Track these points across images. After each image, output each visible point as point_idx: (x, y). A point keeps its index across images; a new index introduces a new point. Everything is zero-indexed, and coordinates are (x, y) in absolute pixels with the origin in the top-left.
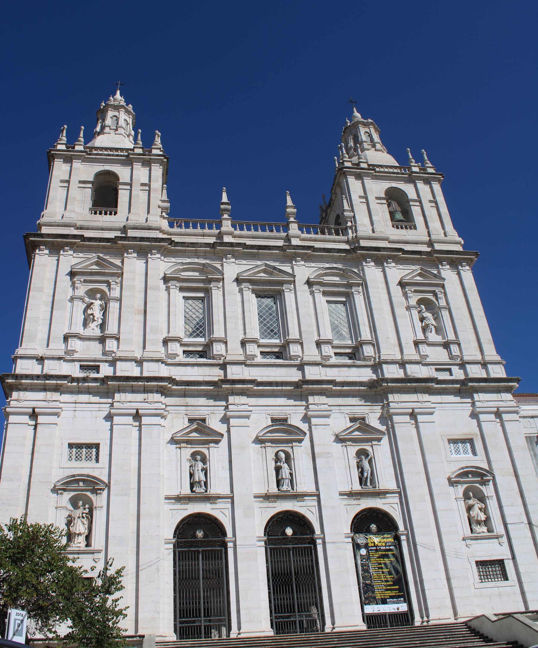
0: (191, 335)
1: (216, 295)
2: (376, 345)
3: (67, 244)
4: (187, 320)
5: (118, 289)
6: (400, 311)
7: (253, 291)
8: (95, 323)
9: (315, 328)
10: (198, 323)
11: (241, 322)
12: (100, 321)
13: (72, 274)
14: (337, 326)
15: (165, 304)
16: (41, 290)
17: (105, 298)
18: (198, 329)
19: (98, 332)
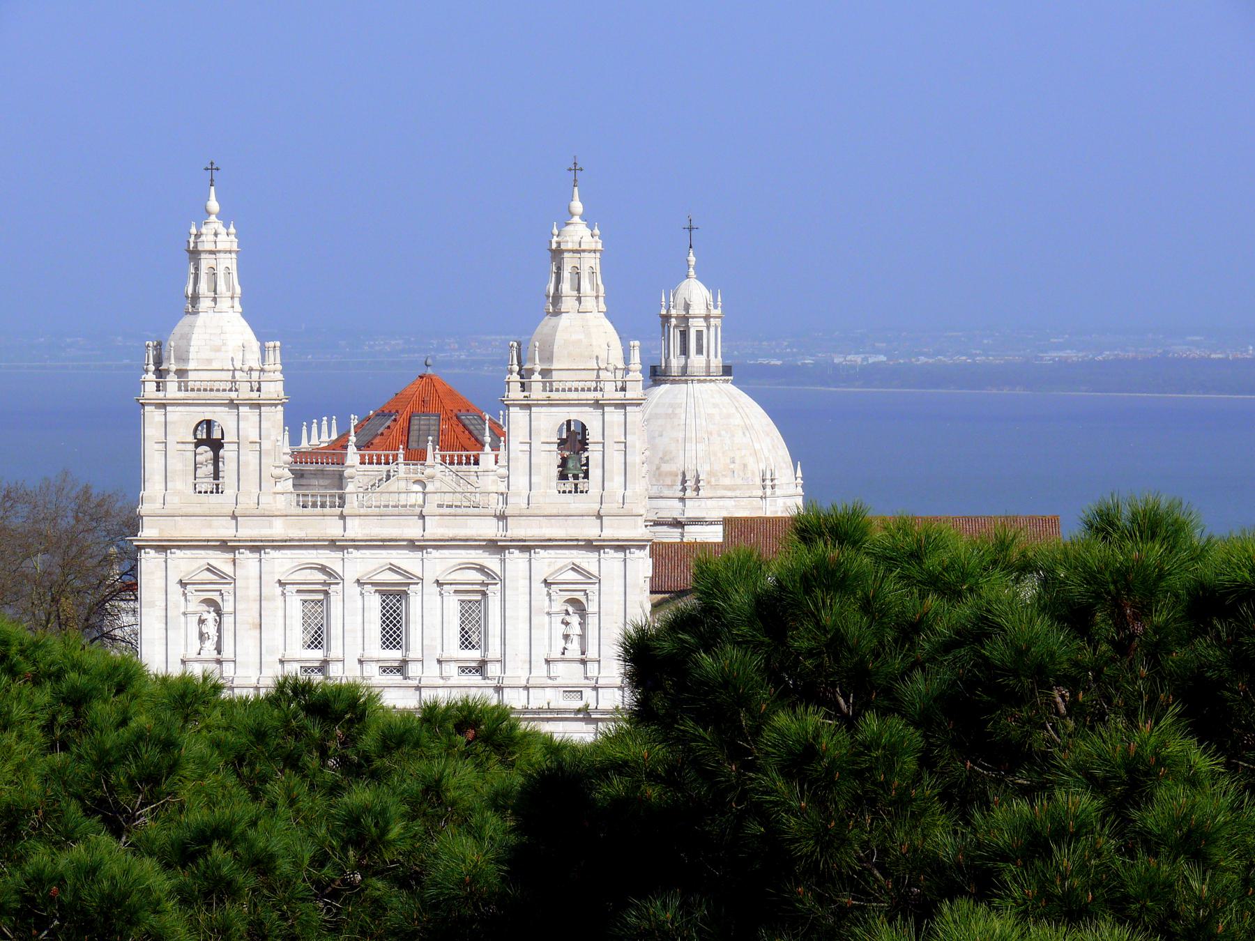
0: (309, 646)
1: (335, 600)
2: (502, 661)
3: (174, 547)
4: (306, 625)
5: (232, 598)
6: (541, 620)
7: (376, 591)
8: (210, 641)
9: (439, 640)
10: (316, 632)
11: (360, 634)
12: (216, 639)
13: (183, 584)
14: (467, 633)
15: (281, 613)
16: (152, 605)
17: (219, 612)
18: (316, 639)
19: (214, 655)
